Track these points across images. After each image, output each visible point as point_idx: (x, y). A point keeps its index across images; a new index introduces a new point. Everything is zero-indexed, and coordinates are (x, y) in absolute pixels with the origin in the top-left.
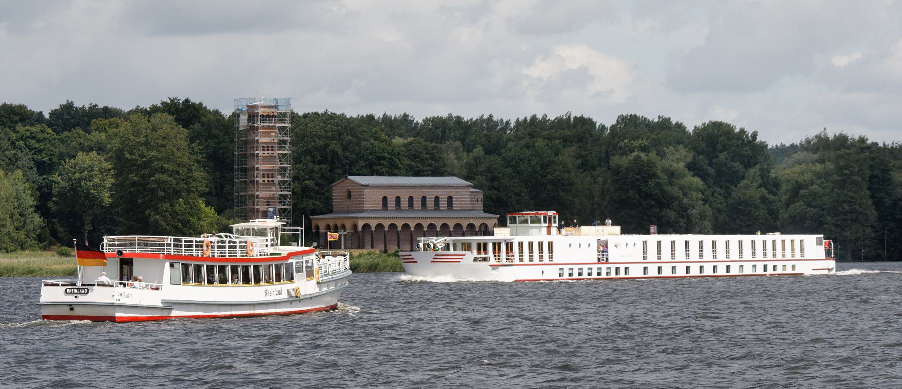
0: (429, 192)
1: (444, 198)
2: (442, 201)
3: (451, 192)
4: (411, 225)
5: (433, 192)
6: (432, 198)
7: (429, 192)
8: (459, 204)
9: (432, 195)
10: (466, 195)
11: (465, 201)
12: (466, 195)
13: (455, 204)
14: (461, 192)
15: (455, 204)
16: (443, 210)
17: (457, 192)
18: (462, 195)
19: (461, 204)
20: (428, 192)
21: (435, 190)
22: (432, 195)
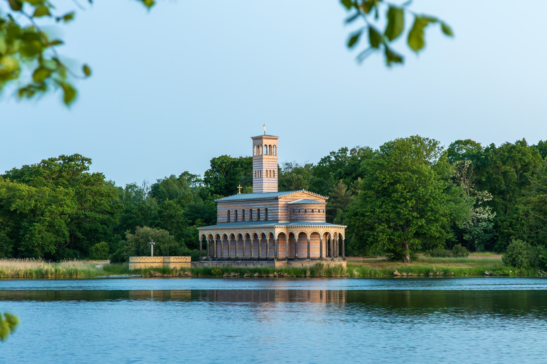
3: (267, 205)
5: (256, 205)
9: (255, 208)
17: (270, 205)
19: (273, 215)
20: (253, 205)
21: (257, 204)
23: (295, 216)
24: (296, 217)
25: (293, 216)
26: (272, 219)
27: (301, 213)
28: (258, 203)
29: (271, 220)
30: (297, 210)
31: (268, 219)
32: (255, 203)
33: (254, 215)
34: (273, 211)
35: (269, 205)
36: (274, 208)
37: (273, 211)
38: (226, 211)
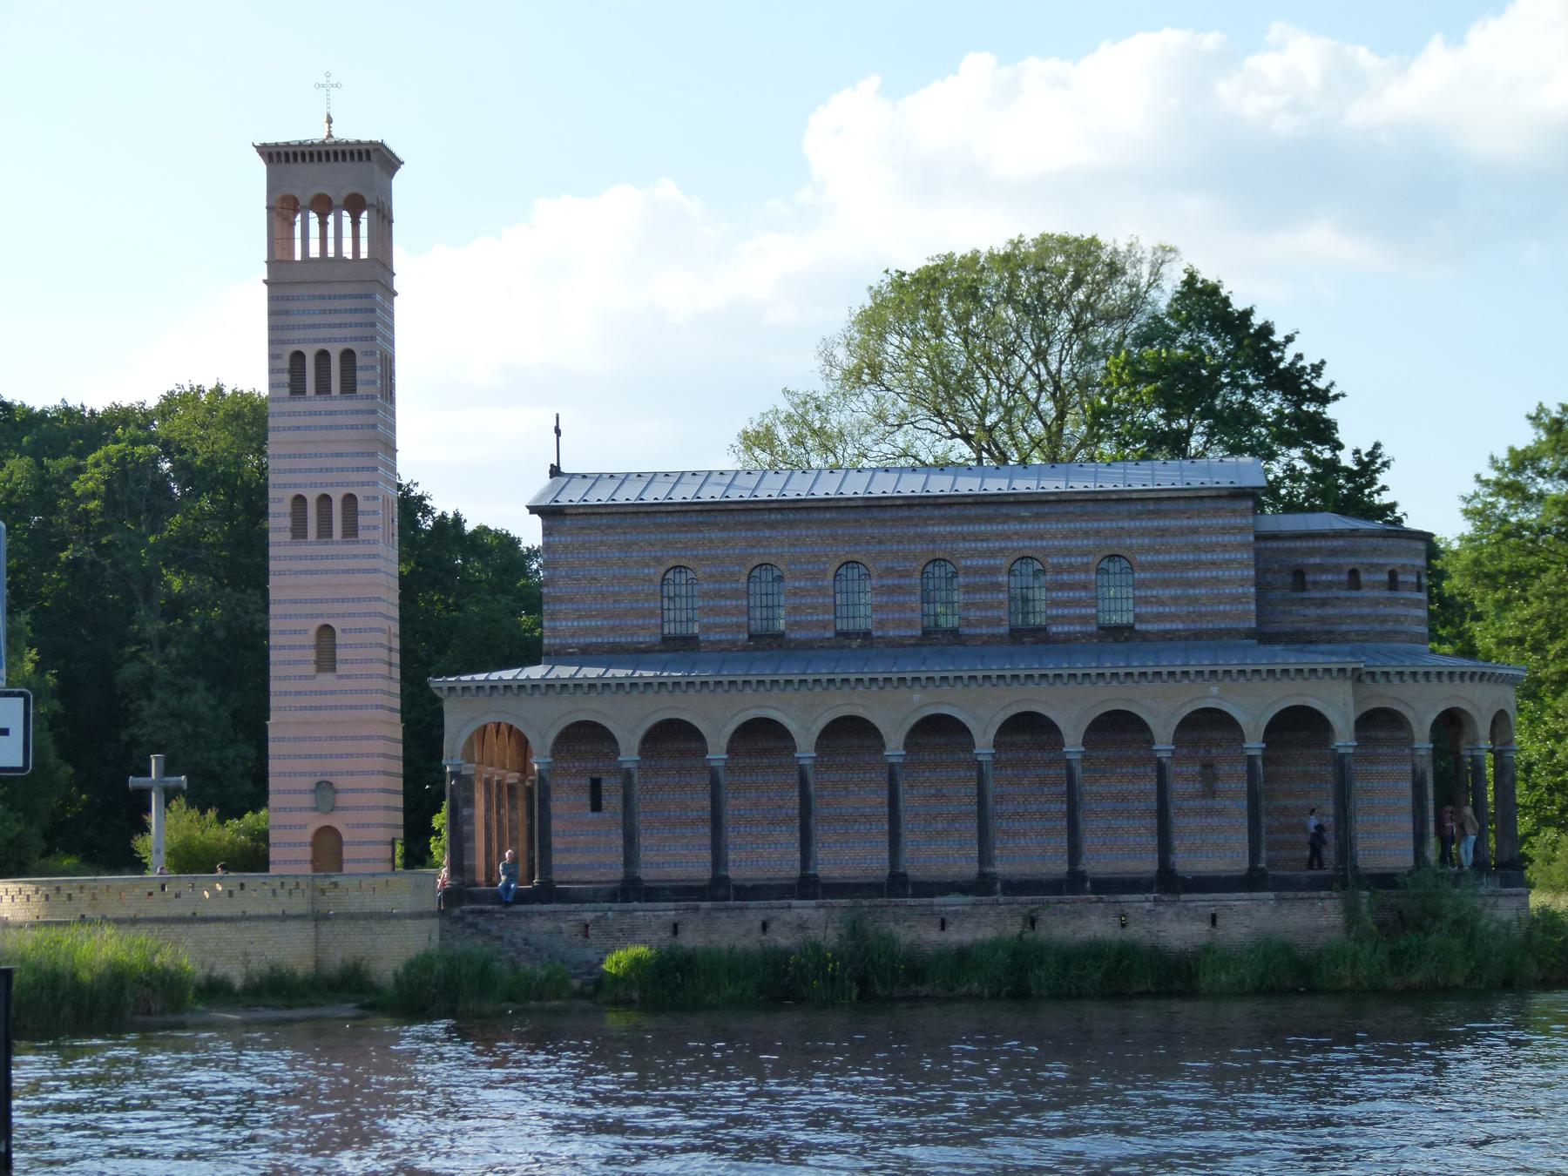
0: (976, 537)
1: (1072, 569)
3: (1119, 533)
5: (999, 536)
6: (993, 570)
7: (976, 537)
8: (1176, 600)
9: (993, 554)
10: (1225, 547)
11: (1218, 580)
12: (1225, 547)
14: (1193, 531)
17: (1162, 532)
18: (1197, 548)
19: (1195, 601)
22: (993, 554)
23: (1313, 612)
25: (1283, 613)
26: (1180, 626)
27: (1367, 593)
28: (1022, 520)
30: (1337, 569)
32: (990, 520)
35: (1145, 532)
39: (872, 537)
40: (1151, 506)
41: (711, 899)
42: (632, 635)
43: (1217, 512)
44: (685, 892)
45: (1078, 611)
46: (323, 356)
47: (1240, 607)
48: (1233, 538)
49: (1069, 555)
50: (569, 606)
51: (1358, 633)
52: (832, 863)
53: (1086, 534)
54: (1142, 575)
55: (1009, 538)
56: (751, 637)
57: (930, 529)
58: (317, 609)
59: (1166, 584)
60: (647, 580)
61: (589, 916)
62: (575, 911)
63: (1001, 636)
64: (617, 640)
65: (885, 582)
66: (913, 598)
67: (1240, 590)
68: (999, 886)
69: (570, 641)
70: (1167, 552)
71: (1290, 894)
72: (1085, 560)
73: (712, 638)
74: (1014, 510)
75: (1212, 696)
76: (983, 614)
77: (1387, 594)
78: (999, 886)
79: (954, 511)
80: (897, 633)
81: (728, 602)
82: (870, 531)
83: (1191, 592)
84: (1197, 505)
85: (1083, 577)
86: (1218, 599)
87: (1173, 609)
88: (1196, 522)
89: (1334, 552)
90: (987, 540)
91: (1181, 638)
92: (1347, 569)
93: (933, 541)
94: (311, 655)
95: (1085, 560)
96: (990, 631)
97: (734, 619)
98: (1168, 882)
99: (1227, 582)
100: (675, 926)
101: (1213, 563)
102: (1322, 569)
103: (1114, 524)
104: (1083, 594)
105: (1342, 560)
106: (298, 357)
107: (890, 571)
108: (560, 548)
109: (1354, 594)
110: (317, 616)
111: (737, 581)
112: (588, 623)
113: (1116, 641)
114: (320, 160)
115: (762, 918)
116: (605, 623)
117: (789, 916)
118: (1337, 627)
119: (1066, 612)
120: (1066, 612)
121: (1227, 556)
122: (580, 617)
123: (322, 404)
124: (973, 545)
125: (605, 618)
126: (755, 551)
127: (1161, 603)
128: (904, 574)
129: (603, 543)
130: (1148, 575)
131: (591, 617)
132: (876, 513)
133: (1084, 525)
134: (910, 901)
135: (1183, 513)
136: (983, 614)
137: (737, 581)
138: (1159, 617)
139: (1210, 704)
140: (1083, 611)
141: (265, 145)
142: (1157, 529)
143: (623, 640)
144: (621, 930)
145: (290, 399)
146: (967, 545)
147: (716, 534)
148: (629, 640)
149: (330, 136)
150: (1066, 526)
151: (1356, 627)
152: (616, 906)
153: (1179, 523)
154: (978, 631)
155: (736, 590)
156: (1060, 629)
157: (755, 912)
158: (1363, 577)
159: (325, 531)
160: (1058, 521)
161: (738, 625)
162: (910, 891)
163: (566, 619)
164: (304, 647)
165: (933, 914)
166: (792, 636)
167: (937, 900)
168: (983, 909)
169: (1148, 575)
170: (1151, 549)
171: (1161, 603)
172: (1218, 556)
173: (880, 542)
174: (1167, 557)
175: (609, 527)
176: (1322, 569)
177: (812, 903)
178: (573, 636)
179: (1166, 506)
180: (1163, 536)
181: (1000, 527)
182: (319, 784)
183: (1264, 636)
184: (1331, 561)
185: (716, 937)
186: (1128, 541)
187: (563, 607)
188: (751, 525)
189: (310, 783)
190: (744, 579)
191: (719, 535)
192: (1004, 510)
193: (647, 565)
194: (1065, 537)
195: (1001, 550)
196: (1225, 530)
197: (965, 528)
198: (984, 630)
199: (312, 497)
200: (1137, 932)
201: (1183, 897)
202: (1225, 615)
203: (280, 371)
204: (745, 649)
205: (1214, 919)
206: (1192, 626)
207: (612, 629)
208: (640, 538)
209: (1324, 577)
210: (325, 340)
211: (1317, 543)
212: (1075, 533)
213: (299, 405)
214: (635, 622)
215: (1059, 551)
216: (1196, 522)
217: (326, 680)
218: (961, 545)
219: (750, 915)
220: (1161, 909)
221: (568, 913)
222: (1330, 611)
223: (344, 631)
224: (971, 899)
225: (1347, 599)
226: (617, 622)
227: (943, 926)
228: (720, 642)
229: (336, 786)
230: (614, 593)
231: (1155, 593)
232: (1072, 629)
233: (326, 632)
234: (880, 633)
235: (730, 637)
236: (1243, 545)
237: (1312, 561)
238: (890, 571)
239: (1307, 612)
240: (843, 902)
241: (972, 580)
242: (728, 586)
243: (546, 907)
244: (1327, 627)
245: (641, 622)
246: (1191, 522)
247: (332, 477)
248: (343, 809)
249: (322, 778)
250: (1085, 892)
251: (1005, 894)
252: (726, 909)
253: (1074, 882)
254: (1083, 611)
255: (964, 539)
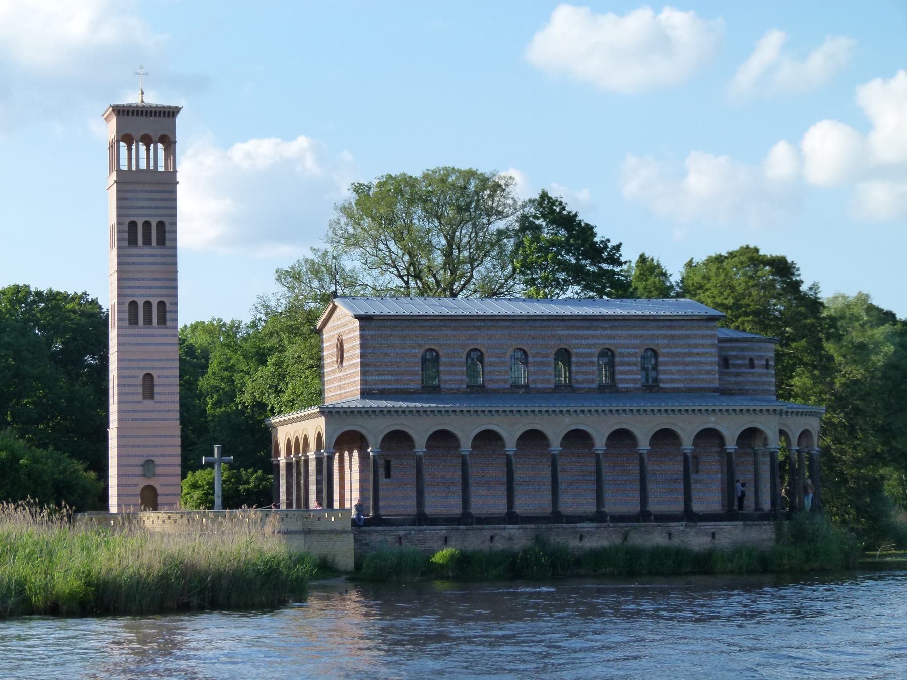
1: (630, 355)
2: (623, 364)
3: (652, 337)
4: (504, 433)
5: (593, 337)
6: (590, 355)
8: (679, 372)
9: (590, 346)
10: (703, 346)
11: (700, 363)
12: (703, 346)
13: (665, 372)
14: (688, 337)
15: (665, 372)
16: (628, 391)
17: (673, 337)
18: (690, 345)
19: (688, 373)
21: (598, 332)
22: (590, 346)
23: (732, 379)
24: (736, 383)
26: (682, 386)
27: (757, 370)
28: (605, 329)
29: (676, 391)
30: (743, 358)
31: (661, 385)
32: (588, 328)
33: (583, 369)
34: (688, 359)
35: (665, 337)
36: (695, 350)
37: (688, 359)
38: (419, 352)
39: (530, 336)
40: (668, 324)
41: (464, 525)
42: (406, 384)
43: (700, 328)
44: (450, 521)
45: (632, 377)
46: (147, 224)
47: (711, 376)
48: (707, 341)
49: (628, 347)
50: (374, 368)
51: (754, 390)
52: (524, 504)
53: (636, 337)
54: (663, 359)
55: (598, 338)
56: (468, 387)
57: (559, 333)
58: (142, 364)
59: (675, 363)
60: (414, 355)
61: (402, 533)
62: (395, 531)
63: (594, 389)
64: (399, 387)
65: (536, 359)
66: (550, 368)
67: (711, 368)
68: (608, 518)
69: (374, 387)
70: (676, 347)
71: (751, 523)
72: (635, 350)
73: (448, 387)
74: (601, 324)
75: (711, 422)
76: (585, 377)
77: (765, 371)
78: (608, 518)
79: (571, 323)
80: (542, 386)
81: (456, 368)
82: (528, 332)
83: (687, 368)
84: (690, 324)
85: (634, 359)
86: (700, 372)
87: (678, 377)
88: (689, 332)
89: (742, 349)
90: (587, 339)
91: (682, 392)
92: (748, 358)
93: (560, 339)
94: (140, 390)
95: (635, 350)
96: (589, 386)
97: (459, 377)
98: (690, 516)
99: (705, 364)
100: (446, 538)
101: (698, 354)
102: (736, 357)
103: (650, 332)
104: (634, 368)
105: (746, 353)
106: (133, 224)
107: (538, 354)
108: (369, 338)
109: (752, 370)
110: (144, 368)
111: (461, 357)
112: (383, 378)
113: (651, 392)
114: (160, 116)
115: (491, 534)
116: (393, 378)
117: (505, 533)
118: (744, 387)
119: (626, 377)
120: (626, 377)
121: (704, 350)
122: (379, 375)
123: (147, 251)
124: (580, 341)
125: (392, 375)
126: (470, 341)
127: (672, 373)
128: (546, 356)
129: (391, 336)
130: (666, 359)
131: (384, 375)
132: (531, 323)
133: (635, 333)
134: (565, 526)
135: (683, 327)
136: (585, 377)
137: (461, 357)
138: (672, 381)
139: (710, 426)
140: (634, 377)
141: (117, 106)
142: (671, 336)
143: (402, 387)
144: (418, 541)
145: (129, 248)
146: (577, 341)
147: (449, 332)
148: (405, 387)
149: (142, 101)
150: (625, 333)
151: (752, 388)
152: (416, 528)
153: (681, 333)
154: (582, 386)
155: (460, 362)
156: (623, 386)
157: (487, 531)
158: (756, 362)
159: (148, 321)
160: (622, 330)
161: (462, 381)
162: (564, 520)
163: (372, 375)
164: (137, 385)
165: (577, 533)
166: (489, 387)
167: (579, 525)
168: (602, 530)
169: (666, 359)
170: (668, 346)
171: (672, 373)
172: (701, 350)
173: (533, 338)
174: (676, 350)
175: (395, 327)
176: (736, 357)
177: (517, 526)
178: (375, 384)
179: (674, 324)
180: (673, 339)
181: (593, 332)
182: (146, 461)
183: (723, 392)
184: (740, 354)
185: (467, 544)
186: (656, 341)
187: (370, 369)
188: (468, 328)
189: (141, 461)
190: (464, 356)
191: (451, 333)
192: (595, 324)
193: (414, 348)
194: (626, 338)
195: (594, 344)
196: (703, 337)
197: (576, 332)
198: (585, 386)
199: (140, 302)
200: (676, 542)
201: (699, 524)
202: (703, 380)
203: (124, 231)
204: (465, 393)
205: (713, 535)
206: (688, 386)
207: (396, 381)
208: (411, 333)
209: (738, 362)
210: (134, 215)
211: (734, 344)
212: (631, 337)
213: (133, 251)
214: (408, 378)
215: (623, 346)
216: (689, 332)
217: (148, 404)
218: (574, 341)
219: (485, 533)
220: (688, 530)
221: (391, 531)
222: (741, 379)
223: (159, 377)
224: (595, 525)
225: (749, 373)
226: (399, 378)
227: (581, 538)
228: (452, 389)
229: (155, 463)
230: (397, 362)
231: (669, 368)
232: (629, 386)
233: (148, 377)
234: (533, 386)
235: (457, 386)
236: (713, 345)
237: (732, 353)
238: (538, 354)
239: (729, 379)
240: (532, 526)
241: (580, 359)
242: (456, 359)
243: (380, 528)
244: (739, 387)
245: (411, 378)
246: (687, 332)
247: (153, 292)
248: (158, 475)
249: (147, 459)
250: (651, 521)
251: (612, 522)
252: (472, 529)
253: (644, 516)
254: (634, 377)
255: (576, 338)
